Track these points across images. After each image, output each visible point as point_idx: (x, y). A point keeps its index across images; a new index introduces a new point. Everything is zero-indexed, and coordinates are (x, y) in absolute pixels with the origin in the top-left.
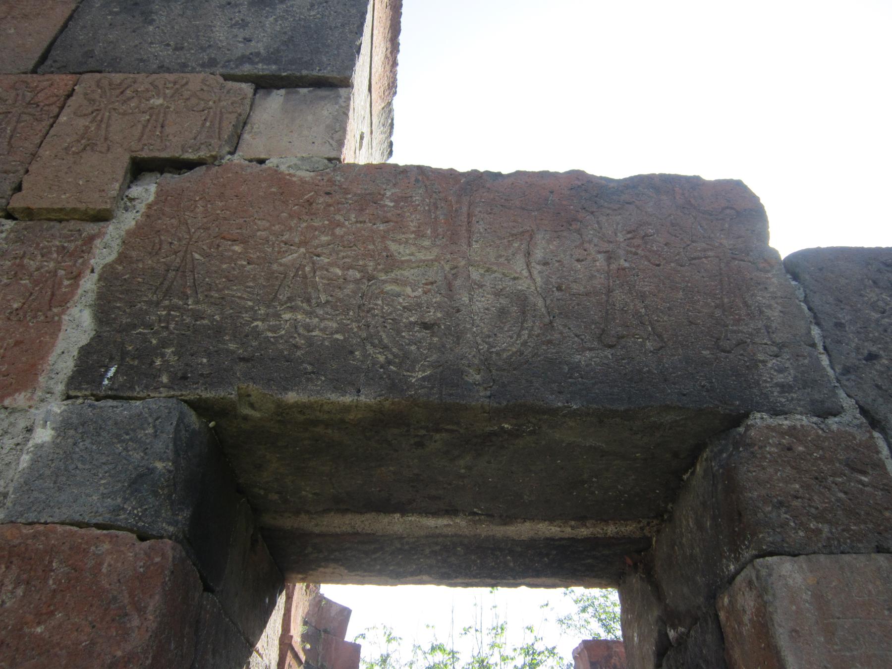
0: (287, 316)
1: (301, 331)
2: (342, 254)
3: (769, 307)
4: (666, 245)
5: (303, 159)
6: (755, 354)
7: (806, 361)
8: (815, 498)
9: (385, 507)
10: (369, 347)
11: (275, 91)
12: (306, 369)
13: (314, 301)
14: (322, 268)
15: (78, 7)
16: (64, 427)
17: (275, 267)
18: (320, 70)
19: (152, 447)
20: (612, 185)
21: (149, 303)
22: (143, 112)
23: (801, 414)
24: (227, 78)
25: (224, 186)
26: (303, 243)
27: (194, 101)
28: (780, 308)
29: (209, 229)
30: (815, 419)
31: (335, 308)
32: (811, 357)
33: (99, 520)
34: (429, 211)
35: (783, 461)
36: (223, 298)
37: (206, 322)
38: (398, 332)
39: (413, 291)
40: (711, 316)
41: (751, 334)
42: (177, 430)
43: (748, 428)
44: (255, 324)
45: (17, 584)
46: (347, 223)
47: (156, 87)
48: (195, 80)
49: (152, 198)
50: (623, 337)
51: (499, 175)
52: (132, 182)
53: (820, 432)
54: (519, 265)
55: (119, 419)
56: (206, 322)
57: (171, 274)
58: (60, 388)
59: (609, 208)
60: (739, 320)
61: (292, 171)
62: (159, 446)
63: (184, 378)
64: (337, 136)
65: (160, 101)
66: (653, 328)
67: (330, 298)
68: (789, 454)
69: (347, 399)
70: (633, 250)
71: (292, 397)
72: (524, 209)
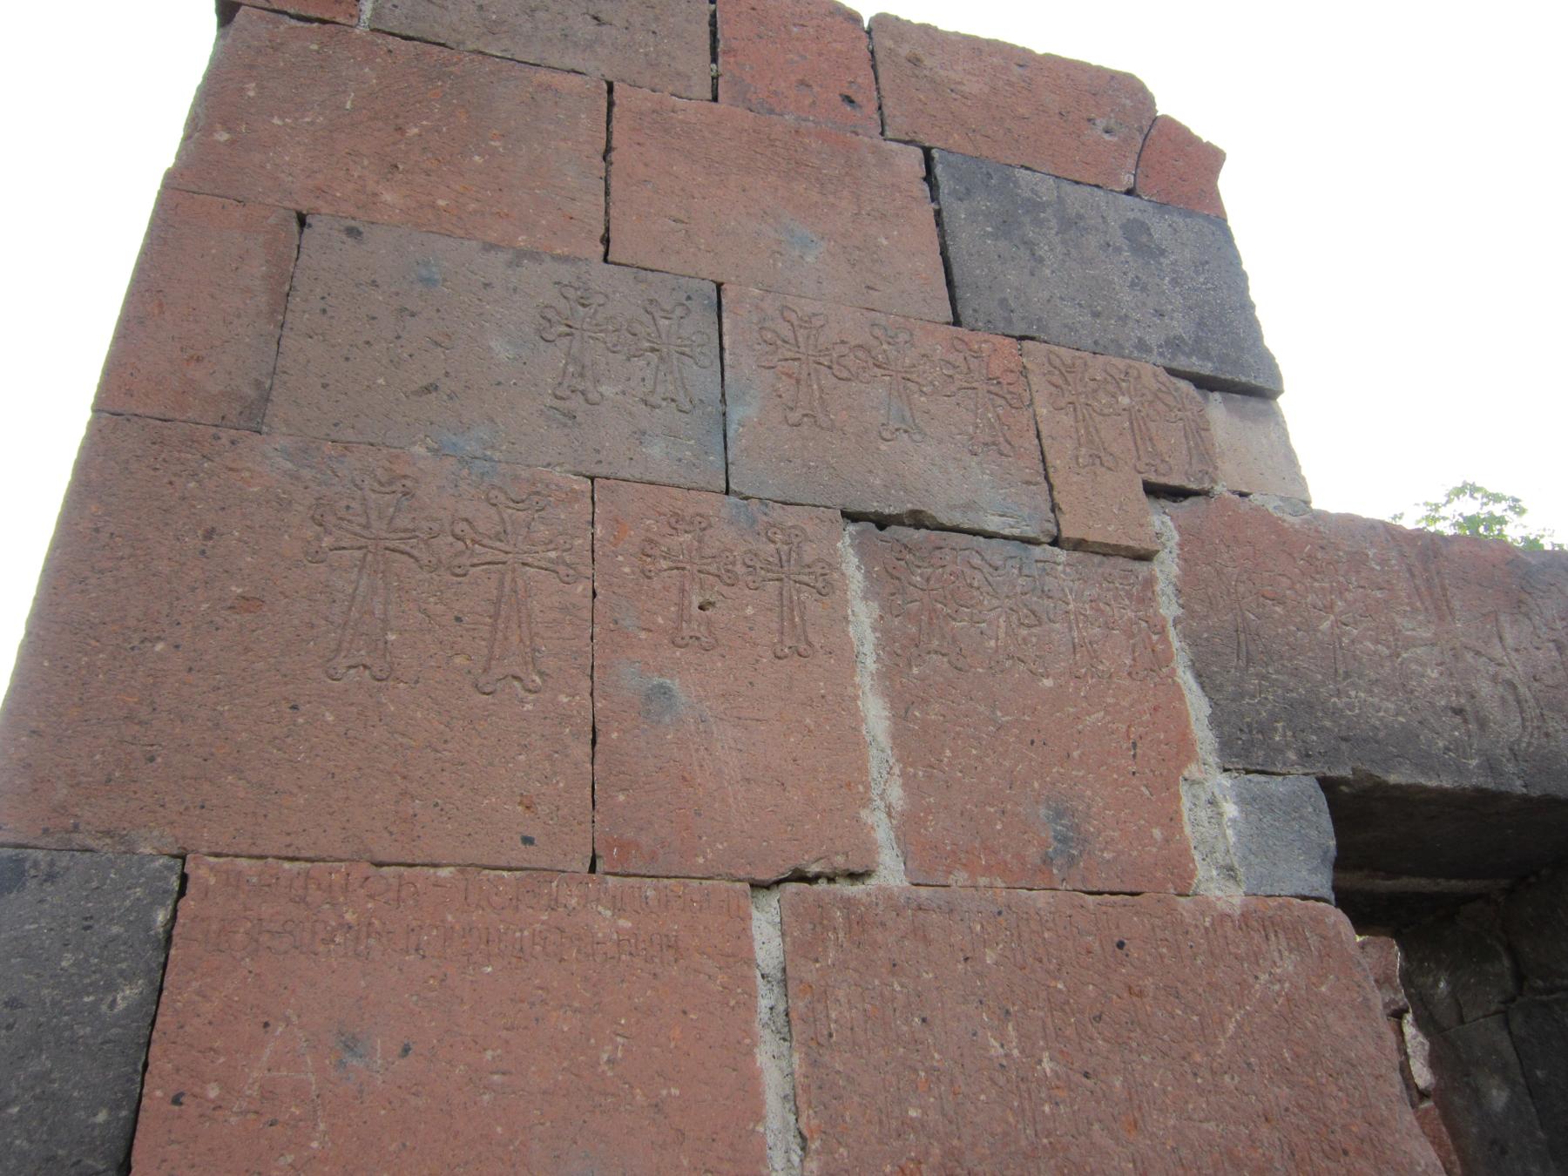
15: (938, 213)
16: (1241, 801)
24: (1172, 372)
45: (1291, 951)
49: (1177, 538)
57: (1242, 637)
58: (1213, 759)
69: (1433, 783)
71: (1393, 779)
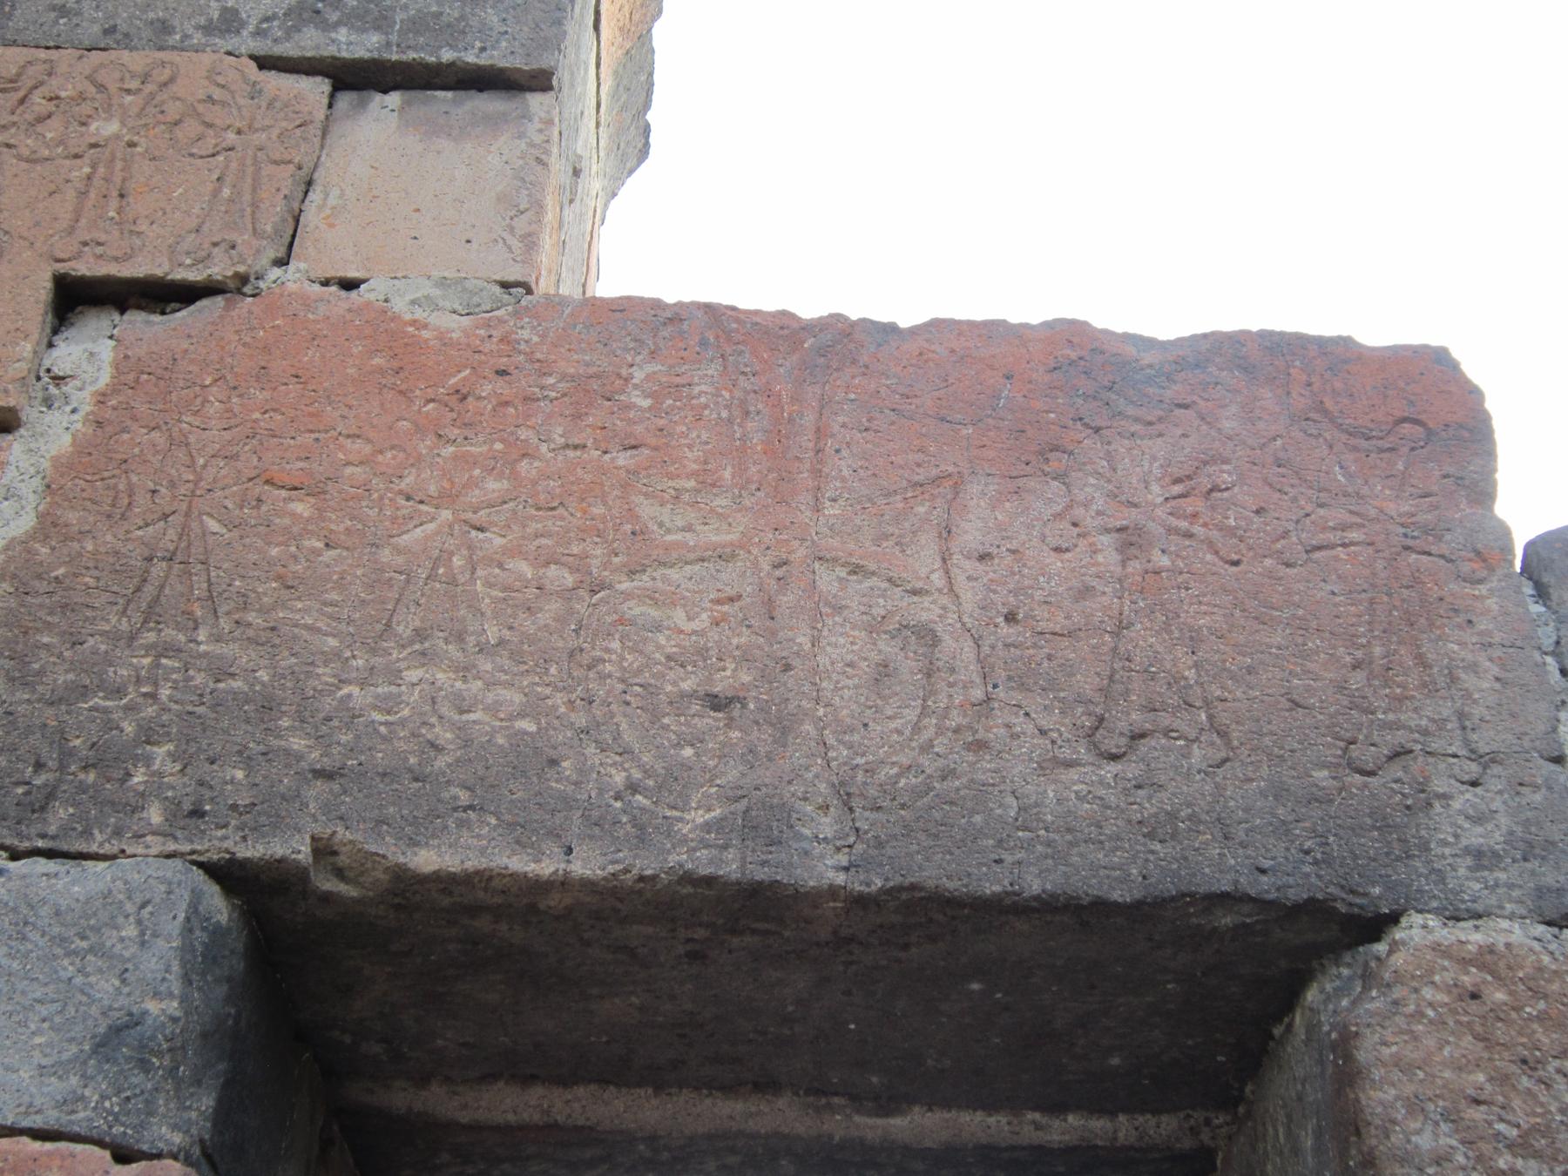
0: (413, 675)
1: (445, 710)
2: (533, 527)
3: (1473, 668)
4: (1257, 512)
5: (443, 283)
6: (1427, 779)
7: (1538, 797)
8: (1516, 1103)
9: (617, 1072)
10: (591, 750)
11: (378, 98)
12: (455, 798)
13: (471, 640)
14: (490, 561)
17: (385, 555)
18: (483, 49)
19: (136, 968)
20: (1147, 358)
21: (113, 637)
22: (77, 156)
23: (1511, 917)
24: (265, 63)
25: (266, 349)
26: (447, 498)
27: (191, 127)
28: (1495, 670)
29: (235, 457)
30: (1541, 929)
31: (517, 657)
32: (1550, 788)
33: (36, 1121)
34: (730, 421)
35: (1458, 1022)
36: (273, 629)
37: (237, 684)
38: (656, 717)
39: (690, 619)
40: (1341, 687)
41: (1425, 732)
42: (188, 929)
43: (1394, 947)
44: (345, 691)
46: (544, 448)
47: (101, 88)
48: (196, 71)
49: (105, 378)
50: (1142, 736)
51: (891, 329)
52: (55, 332)
53: (1546, 959)
54: (923, 561)
55: (64, 904)
56: (237, 684)
57: (158, 569)
59: (1137, 420)
60: (1400, 700)
61: (419, 314)
62: (151, 964)
63: (197, 813)
64: (521, 224)
65: (112, 127)
66: (1211, 717)
67: (506, 633)
68: (1474, 1006)
69: (546, 868)
70: (1184, 524)
71: (426, 860)
72: (942, 419)
